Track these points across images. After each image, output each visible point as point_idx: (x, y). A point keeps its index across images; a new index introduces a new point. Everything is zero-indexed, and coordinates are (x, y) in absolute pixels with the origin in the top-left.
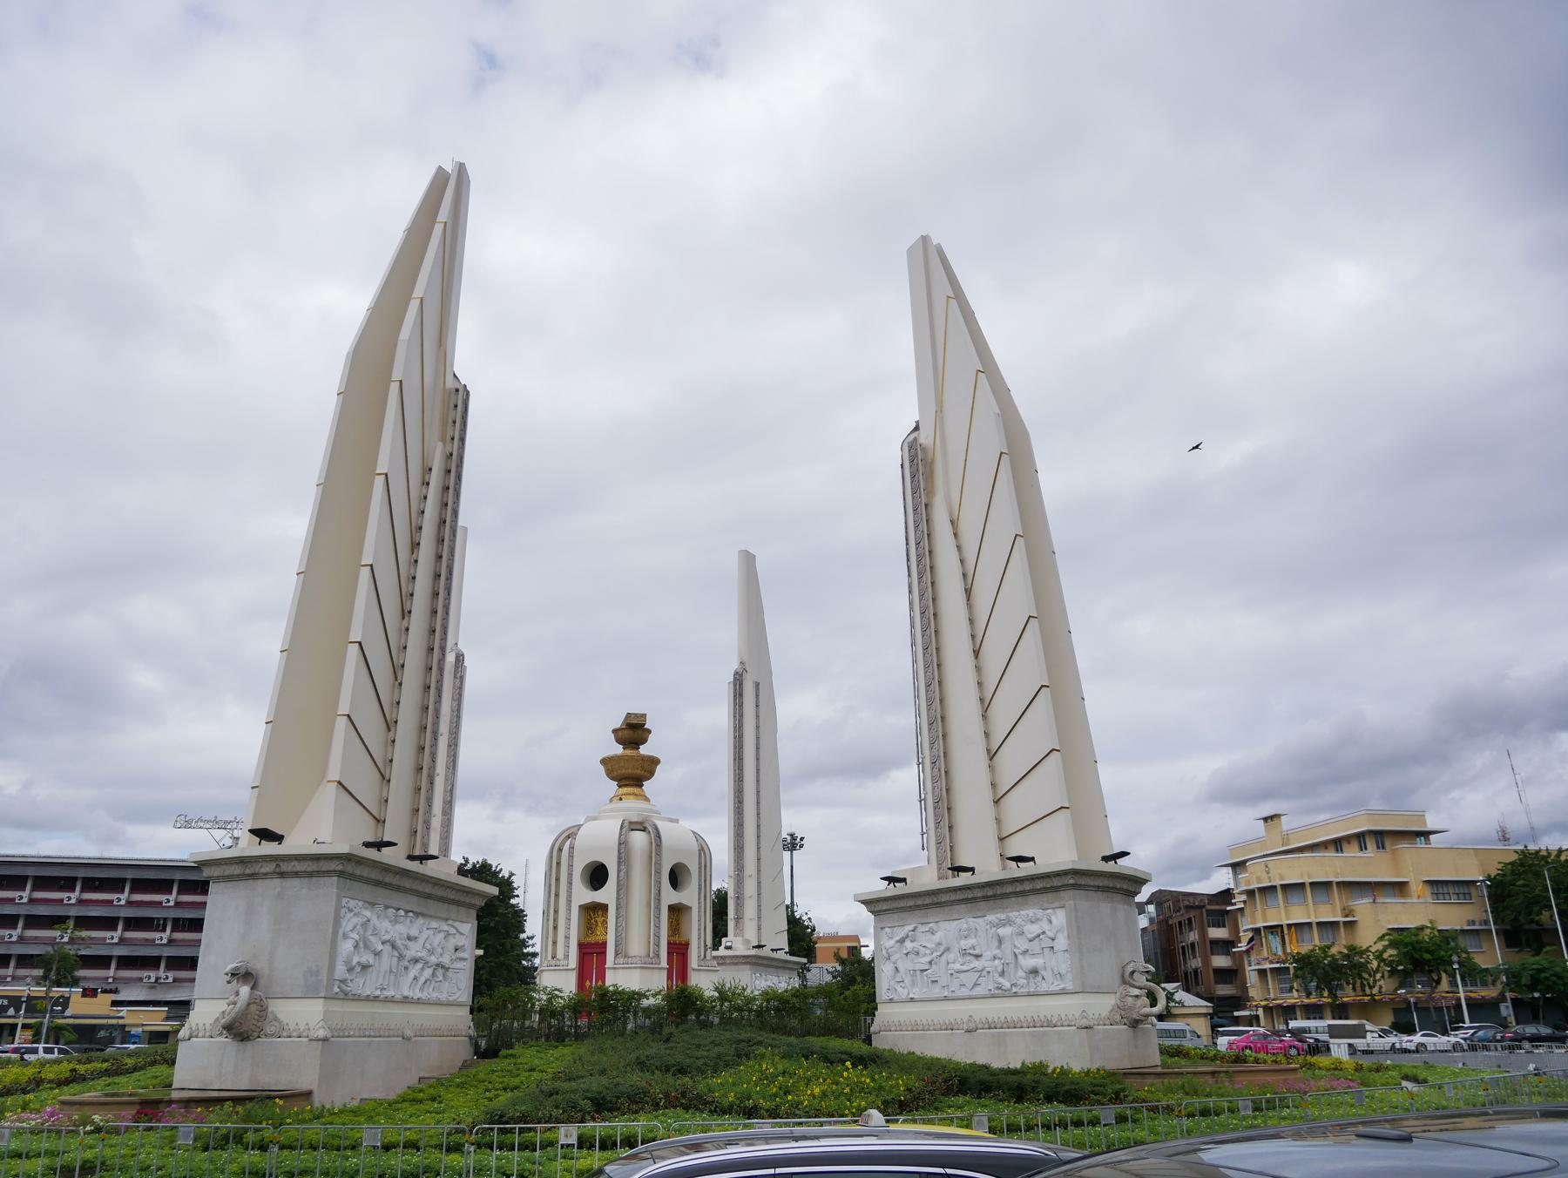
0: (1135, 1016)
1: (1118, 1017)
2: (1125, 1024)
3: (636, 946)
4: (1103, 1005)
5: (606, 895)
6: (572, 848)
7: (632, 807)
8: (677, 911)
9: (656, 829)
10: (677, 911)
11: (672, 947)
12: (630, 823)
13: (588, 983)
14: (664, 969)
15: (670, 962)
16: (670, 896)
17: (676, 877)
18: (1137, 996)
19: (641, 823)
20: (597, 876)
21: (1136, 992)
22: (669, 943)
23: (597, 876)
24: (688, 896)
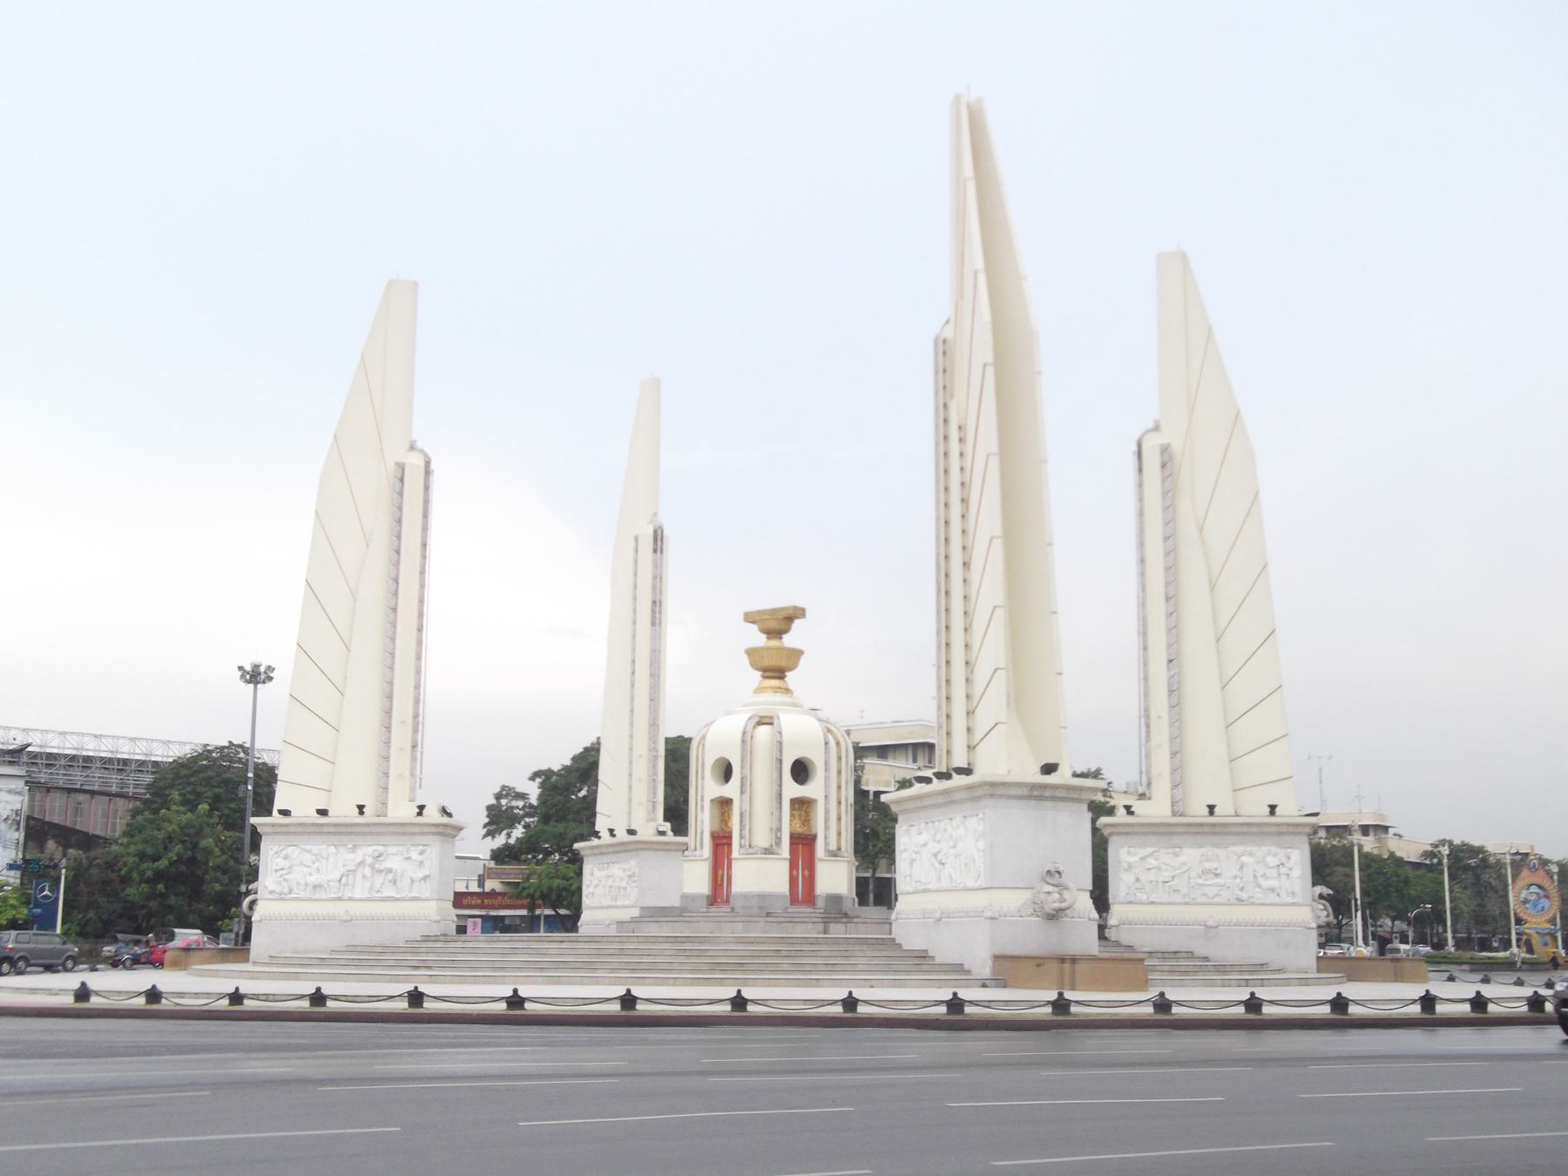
0: (1047, 910)
1: (1030, 911)
2: (1038, 916)
3: (762, 838)
4: (1014, 900)
5: (731, 790)
6: (704, 745)
7: (769, 701)
8: (802, 806)
9: (780, 726)
10: (802, 806)
11: (796, 839)
12: (762, 717)
13: (720, 872)
14: (785, 859)
15: (792, 853)
16: (792, 789)
17: (801, 771)
18: (1049, 893)
19: (771, 717)
20: (726, 772)
21: (1050, 888)
22: (792, 836)
23: (726, 772)
24: (812, 790)
